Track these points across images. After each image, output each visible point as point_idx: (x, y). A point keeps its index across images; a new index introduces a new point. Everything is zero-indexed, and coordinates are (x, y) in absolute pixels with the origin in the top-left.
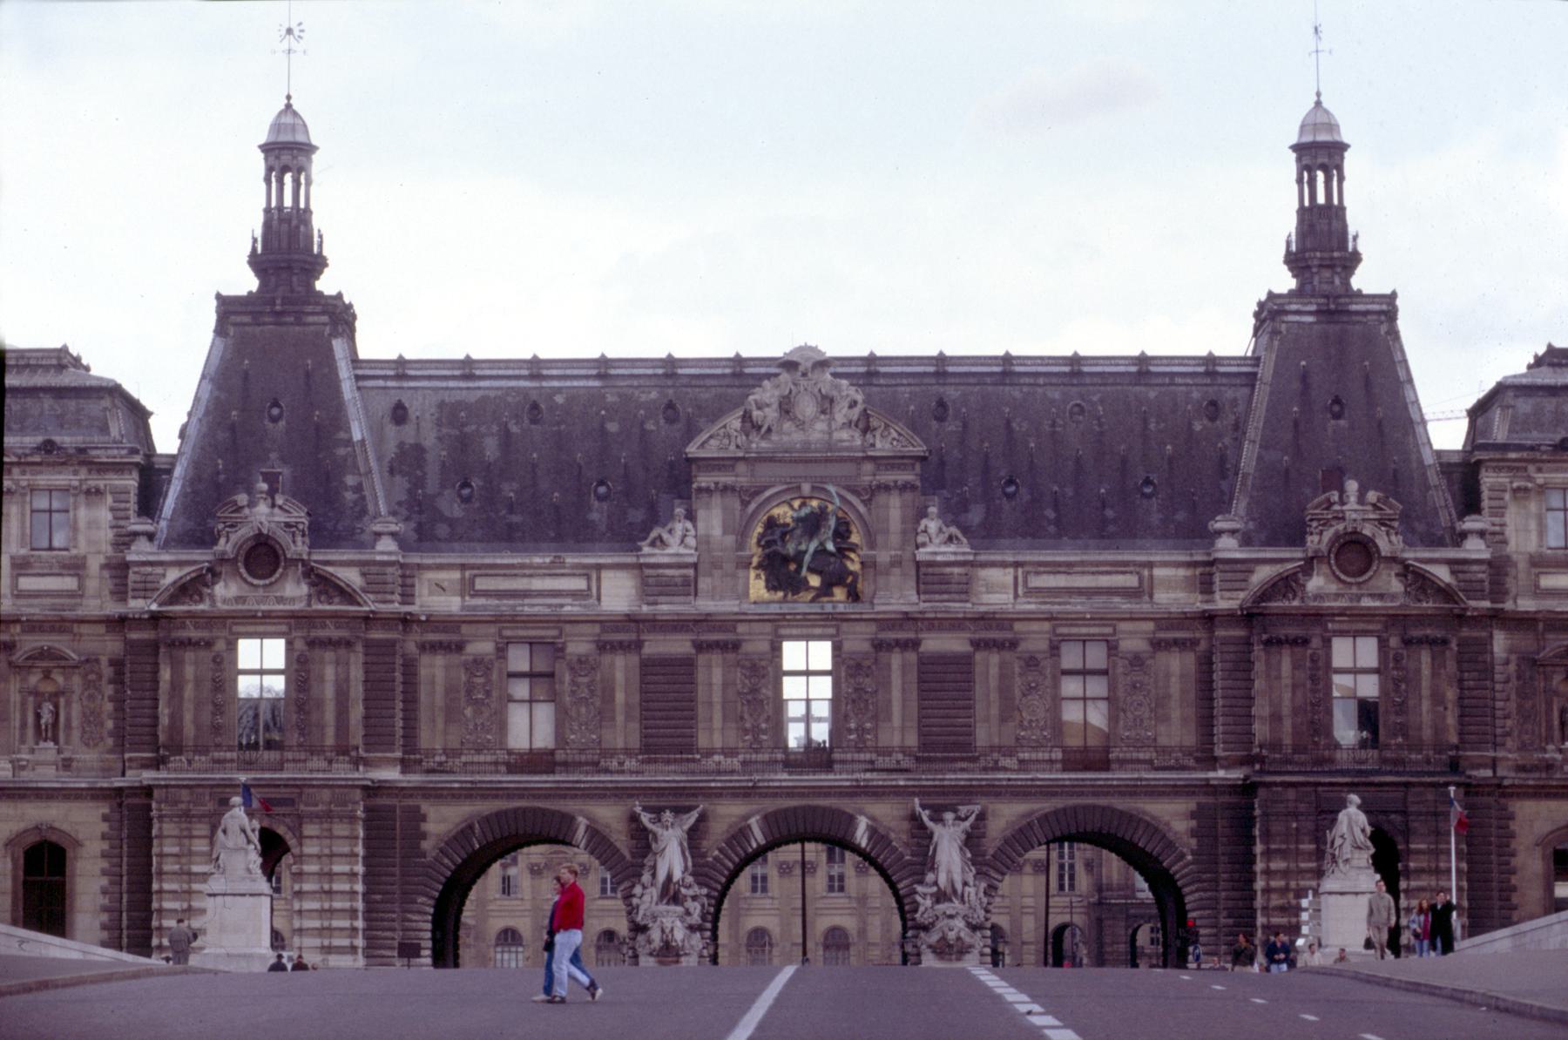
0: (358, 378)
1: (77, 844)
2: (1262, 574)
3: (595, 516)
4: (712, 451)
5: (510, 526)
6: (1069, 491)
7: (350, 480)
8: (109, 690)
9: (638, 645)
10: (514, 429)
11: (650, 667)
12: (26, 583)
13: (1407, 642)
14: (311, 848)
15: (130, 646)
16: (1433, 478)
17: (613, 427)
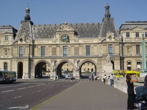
0: (31, 27)
1: (8, 63)
2: (102, 40)
3: (49, 36)
4: (58, 30)
5: (42, 37)
6: (87, 34)
7: (30, 34)
8: (11, 51)
9: (51, 47)
10: (43, 30)
11: (53, 48)
12: (5, 43)
13: (115, 45)
14: (24, 63)
15: (12, 47)
16: (117, 32)
17: (51, 30)
